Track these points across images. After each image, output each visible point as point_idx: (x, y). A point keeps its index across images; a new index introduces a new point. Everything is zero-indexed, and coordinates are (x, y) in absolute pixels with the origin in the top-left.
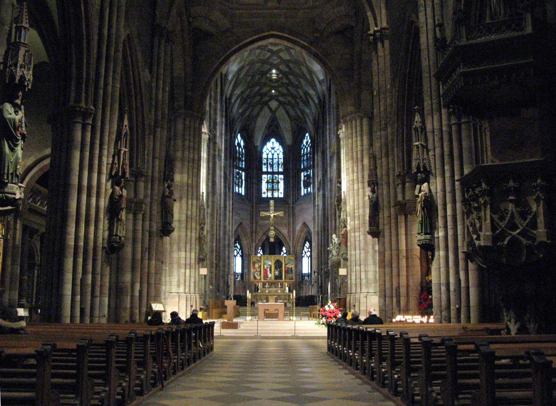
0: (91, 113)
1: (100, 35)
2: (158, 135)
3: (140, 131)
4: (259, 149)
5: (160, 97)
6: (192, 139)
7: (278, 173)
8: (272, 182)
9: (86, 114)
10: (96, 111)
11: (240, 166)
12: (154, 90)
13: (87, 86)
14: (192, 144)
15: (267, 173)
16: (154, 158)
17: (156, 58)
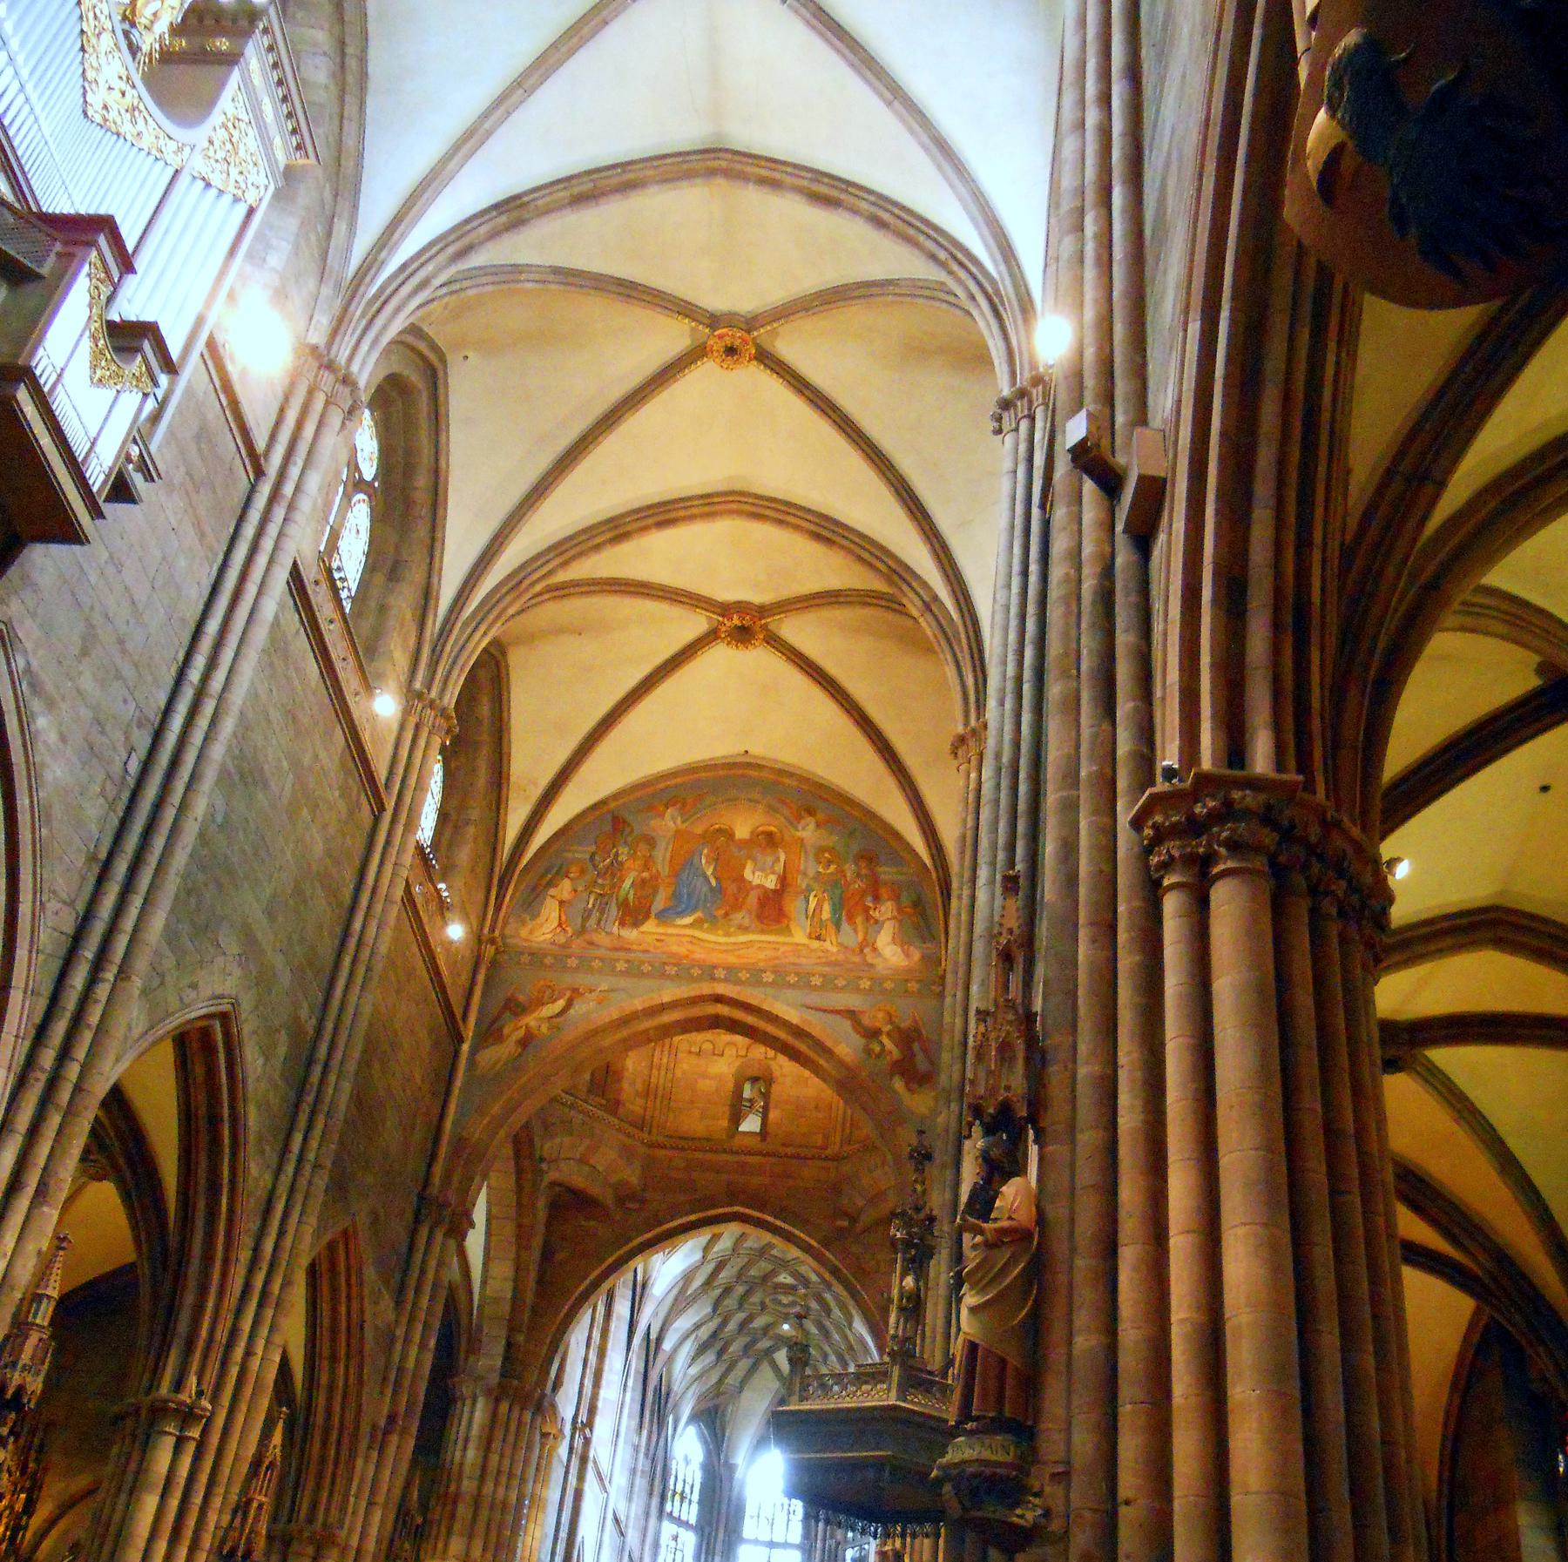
0: (202, 1417)
1: (257, 1249)
2: (391, 1450)
3: (346, 1441)
4: (738, 1475)
5: (411, 1364)
6: (508, 1452)
7: (786, 1545)
9: (187, 1416)
10: (213, 1413)
11: (684, 1518)
12: (398, 1346)
13: (205, 1356)
14: (507, 1462)
15: (756, 1542)
16: (371, 1504)
17: (415, 1273)
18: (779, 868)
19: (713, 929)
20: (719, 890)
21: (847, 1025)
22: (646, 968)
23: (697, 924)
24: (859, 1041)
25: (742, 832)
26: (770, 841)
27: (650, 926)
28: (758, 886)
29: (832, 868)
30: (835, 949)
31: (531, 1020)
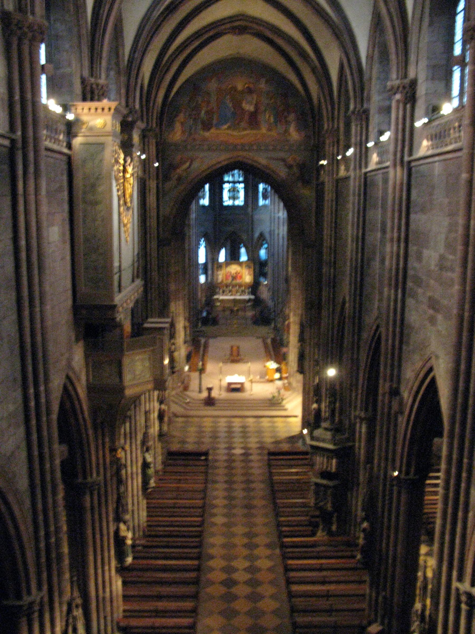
8: (234, 191)
15: (229, 182)
18: (254, 102)
19: (234, 130)
20: (234, 114)
21: (282, 163)
22: (214, 147)
23: (229, 128)
24: (287, 170)
25: (240, 87)
26: (250, 91)
27: (213, 130)
28: (248, 111)
29: (273, 101)
30: (275, 135)
31: (179, 171)
